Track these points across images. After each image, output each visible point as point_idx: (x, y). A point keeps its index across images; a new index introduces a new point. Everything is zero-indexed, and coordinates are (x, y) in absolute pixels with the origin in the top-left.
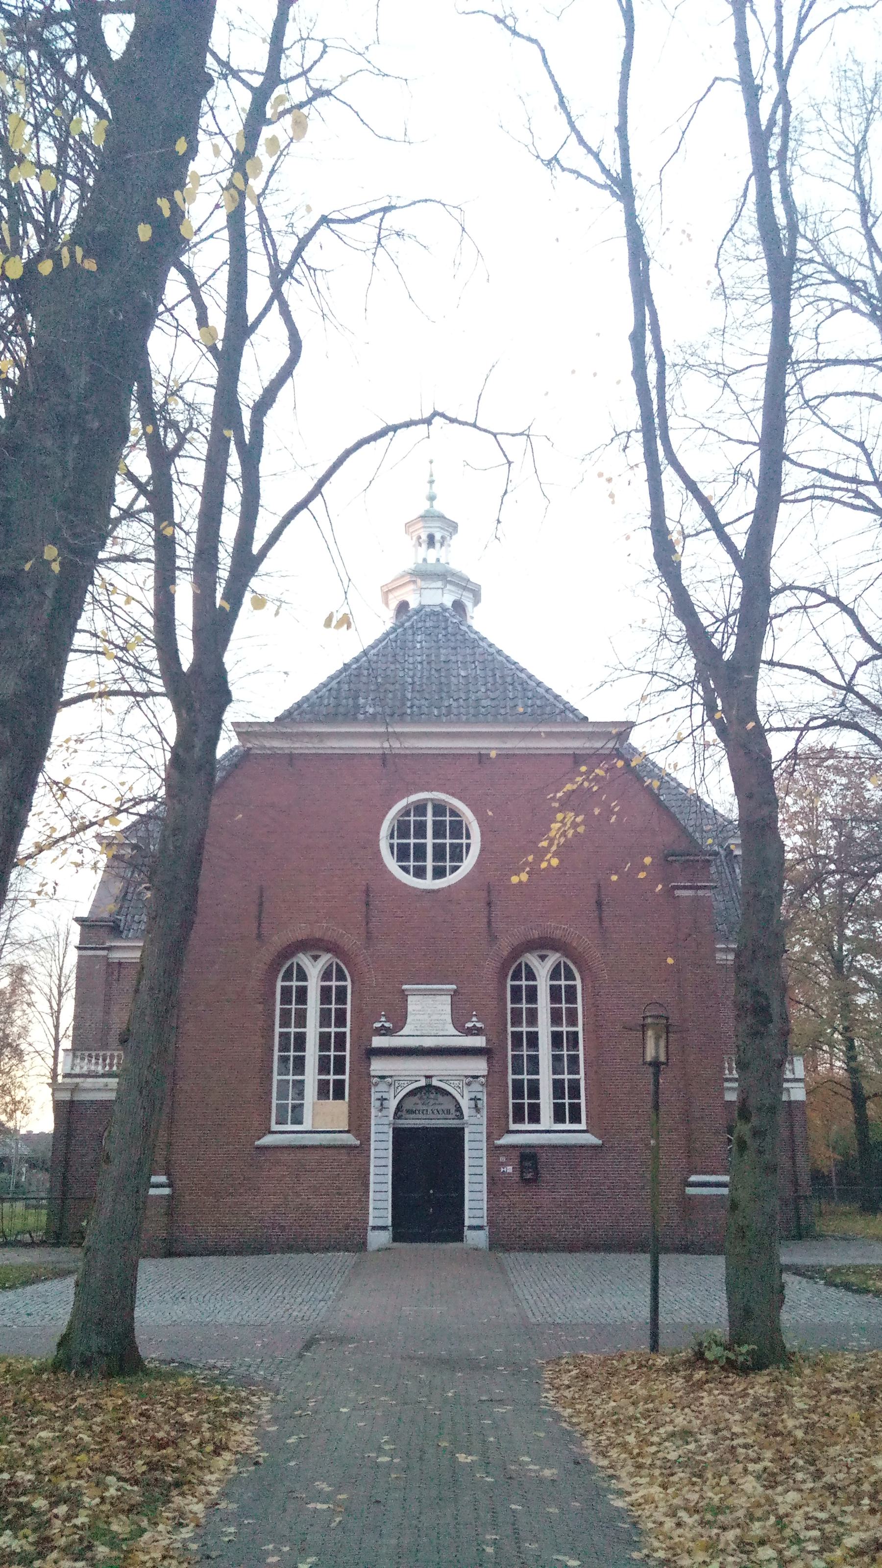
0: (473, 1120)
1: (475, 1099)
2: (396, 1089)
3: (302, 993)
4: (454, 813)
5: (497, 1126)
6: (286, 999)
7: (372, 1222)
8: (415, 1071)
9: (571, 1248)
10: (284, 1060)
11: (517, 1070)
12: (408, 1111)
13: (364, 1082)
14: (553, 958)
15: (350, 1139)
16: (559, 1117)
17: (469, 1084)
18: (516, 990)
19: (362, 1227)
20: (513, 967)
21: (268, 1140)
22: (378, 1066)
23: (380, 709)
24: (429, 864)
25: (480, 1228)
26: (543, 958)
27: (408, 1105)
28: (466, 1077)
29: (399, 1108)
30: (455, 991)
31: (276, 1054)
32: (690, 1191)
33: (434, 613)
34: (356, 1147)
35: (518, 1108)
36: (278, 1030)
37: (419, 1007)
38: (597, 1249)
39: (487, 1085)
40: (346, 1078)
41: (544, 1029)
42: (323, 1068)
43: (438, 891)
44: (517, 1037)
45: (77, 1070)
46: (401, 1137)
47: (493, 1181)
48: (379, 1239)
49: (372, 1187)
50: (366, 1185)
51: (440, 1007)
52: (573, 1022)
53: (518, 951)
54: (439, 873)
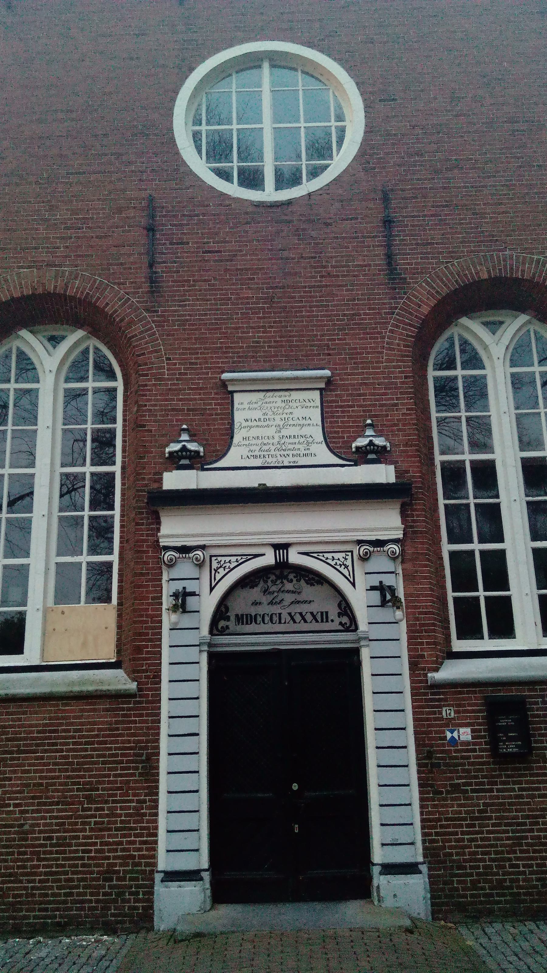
2: (213, 572)
5: (427, 648)
7: (164, 862)
11: (459, 534)
12: (240, 619)
13: (146, 559)
15: (119, 680)
17: (364, 558)
19: (142, 874)
22: (175, 528)
25: (409, 868)
27: (241, 604)
28: (360, 542)
29: (221, 612)
30: (329, 381)
34: (133, 696)
37: (257, 414)
48: (179, 904)
51: (299, 413)
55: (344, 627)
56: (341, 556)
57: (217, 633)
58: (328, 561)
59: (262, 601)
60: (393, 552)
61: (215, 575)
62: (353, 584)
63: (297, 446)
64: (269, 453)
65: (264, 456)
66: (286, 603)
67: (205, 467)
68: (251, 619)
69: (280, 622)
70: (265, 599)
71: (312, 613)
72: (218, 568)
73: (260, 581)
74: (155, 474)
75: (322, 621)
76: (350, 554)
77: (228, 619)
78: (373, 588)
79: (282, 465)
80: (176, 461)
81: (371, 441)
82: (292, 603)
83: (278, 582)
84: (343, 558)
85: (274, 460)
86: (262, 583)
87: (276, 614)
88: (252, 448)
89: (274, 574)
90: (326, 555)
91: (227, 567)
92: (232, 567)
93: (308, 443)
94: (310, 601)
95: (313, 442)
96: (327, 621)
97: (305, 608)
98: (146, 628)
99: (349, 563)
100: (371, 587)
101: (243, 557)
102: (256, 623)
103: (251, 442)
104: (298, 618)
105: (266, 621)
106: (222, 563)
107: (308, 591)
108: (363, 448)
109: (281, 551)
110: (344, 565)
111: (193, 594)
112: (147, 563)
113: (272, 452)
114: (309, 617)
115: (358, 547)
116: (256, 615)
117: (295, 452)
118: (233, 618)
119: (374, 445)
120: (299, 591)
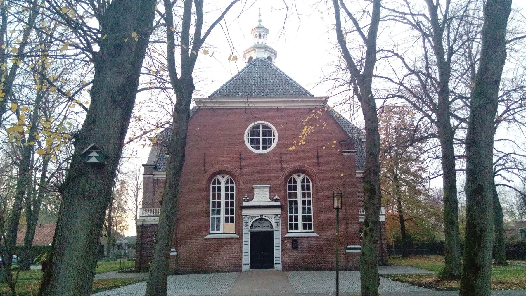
0: (276, 229)
1: (277, 222)
3: (219, 189)
4: (269, 128)
5: (284, 231)
6: (214, 190)
7: (243, 262)
8: (257, 213)
9: (309, 270)
10: (213, 210)
11: (291, 212)
13: (240, 217)
14: (303, 176)
15: (236, 236)
16: (304, 227)
17: (275, 217)
18: (290, 187)
19: (240, 265)
20: (289, 179)
21: (209, 236)
22: (245, 212)
23: (244, 93)
24: (261, 145)
25: (279, 264)
26: (299, 176)
27: (255, 224)
29: (252, 225)
31: (211, 208)
32: (347, 251)
33: (262, 61)
35: (291, 225)
36: (211, 200)
38: (317, 269)
39: (281, 217)
40: (234, 215)
41: (300, 199)
42: (227, 212)
43: (265, 154)
44: (291, 202)
45: (144, 215)
46: (253, 235)
47: (283, 249)
49: (243, 251)
50: (241, 250)
52: (309, 197)
53: (291, 174)
54: (264, 148)
68: (256, 227)
80: (245, 201)
107: (266, 222)
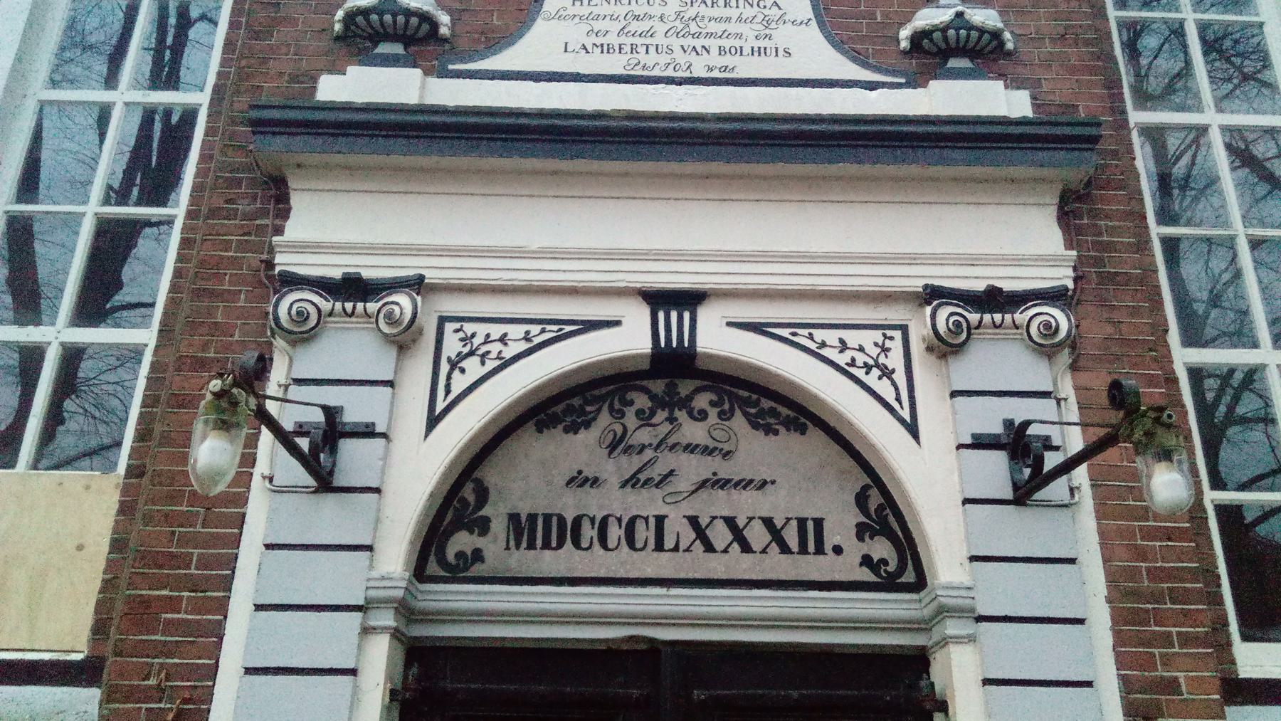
0: (1003, 590)
1: (1018, 444)
8: (582, 265)
12: (525, 530)
17: (946, 348)
28: (933, 295)
55: (877, 574)
56: (869, 339)
57: (443, 574)
58: (825, 352)
59: (603, 476)
60: (1047, 325)
61: (449, 378)
62: (912, 429)
63: (733, 28)
64: (648, 41)
65: (633, 49)
66: (683, 484)
67: (451, 67)
68: (563, 531)
69: (659, 547)
70: (613, 469)
71: (768, 522)
72: (462, 357)
73: (599, 410)
74: (294, 78)
75: (803, 550)
76: (897, 334)
77: (483, 526)
78: (981, 443)
79: (687, 74)
80: (362, 39)
81: (960, 15)
82: (702, 485)
83: (661, 415)
84: (876, 344)
85: (664, 59)
86: (604, 419)
87: (646, 519)
88: (597, 25)
89: (646, 390)
90: (819, 335)
91: (493, 355)
92: (508, 353)
93: (767, 22)
94: (765, 483)
95: (781, 19)
96: (820, 550)
97: (745, 505)
98: (185, 540)
99: (895, 360)
100: (974, 436)
101: (549, 327)
102: (577, 544)
103: (596, 11)
104: (720, 535)
105: (612, 543)
106: (477, 341)
107: (754, 450)
108: (937, 35)
109: (674, 315)
110: (877, 366)
111: (368, 432)
112: (226, 330)
113: (659, 39)
114: (757, 535)
115: (928, 310)
116: (578, 521)
117: (727, 43)
118: (499, 526)
119: (970, 27)
120: (726, 447)
